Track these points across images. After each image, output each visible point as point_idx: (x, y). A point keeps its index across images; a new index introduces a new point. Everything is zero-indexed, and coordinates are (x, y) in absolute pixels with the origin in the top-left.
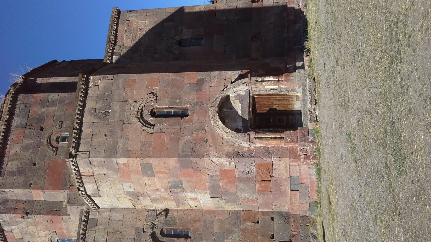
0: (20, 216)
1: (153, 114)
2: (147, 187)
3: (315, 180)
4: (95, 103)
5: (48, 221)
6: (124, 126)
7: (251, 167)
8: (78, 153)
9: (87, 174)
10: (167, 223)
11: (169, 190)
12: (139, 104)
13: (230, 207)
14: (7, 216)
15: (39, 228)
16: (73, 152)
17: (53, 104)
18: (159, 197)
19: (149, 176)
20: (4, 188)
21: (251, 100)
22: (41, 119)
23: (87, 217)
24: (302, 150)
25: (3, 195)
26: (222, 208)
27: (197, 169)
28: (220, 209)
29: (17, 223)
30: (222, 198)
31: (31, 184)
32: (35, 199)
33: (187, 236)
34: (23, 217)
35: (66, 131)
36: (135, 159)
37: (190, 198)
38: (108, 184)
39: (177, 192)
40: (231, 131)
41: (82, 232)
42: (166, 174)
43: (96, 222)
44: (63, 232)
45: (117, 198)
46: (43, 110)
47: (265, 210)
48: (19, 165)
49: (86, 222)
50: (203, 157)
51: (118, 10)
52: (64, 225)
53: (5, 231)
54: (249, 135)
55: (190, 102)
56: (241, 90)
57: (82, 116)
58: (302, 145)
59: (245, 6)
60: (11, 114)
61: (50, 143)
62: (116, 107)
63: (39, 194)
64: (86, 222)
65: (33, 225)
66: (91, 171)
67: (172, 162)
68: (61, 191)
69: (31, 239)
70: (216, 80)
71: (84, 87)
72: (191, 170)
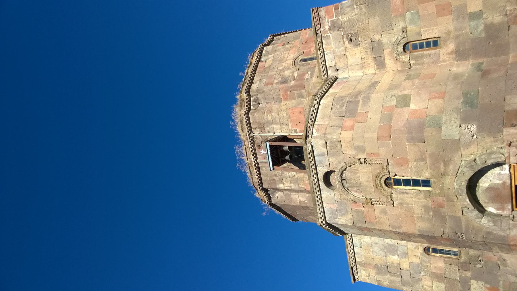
15: (291, 52)
44: (310, 50)
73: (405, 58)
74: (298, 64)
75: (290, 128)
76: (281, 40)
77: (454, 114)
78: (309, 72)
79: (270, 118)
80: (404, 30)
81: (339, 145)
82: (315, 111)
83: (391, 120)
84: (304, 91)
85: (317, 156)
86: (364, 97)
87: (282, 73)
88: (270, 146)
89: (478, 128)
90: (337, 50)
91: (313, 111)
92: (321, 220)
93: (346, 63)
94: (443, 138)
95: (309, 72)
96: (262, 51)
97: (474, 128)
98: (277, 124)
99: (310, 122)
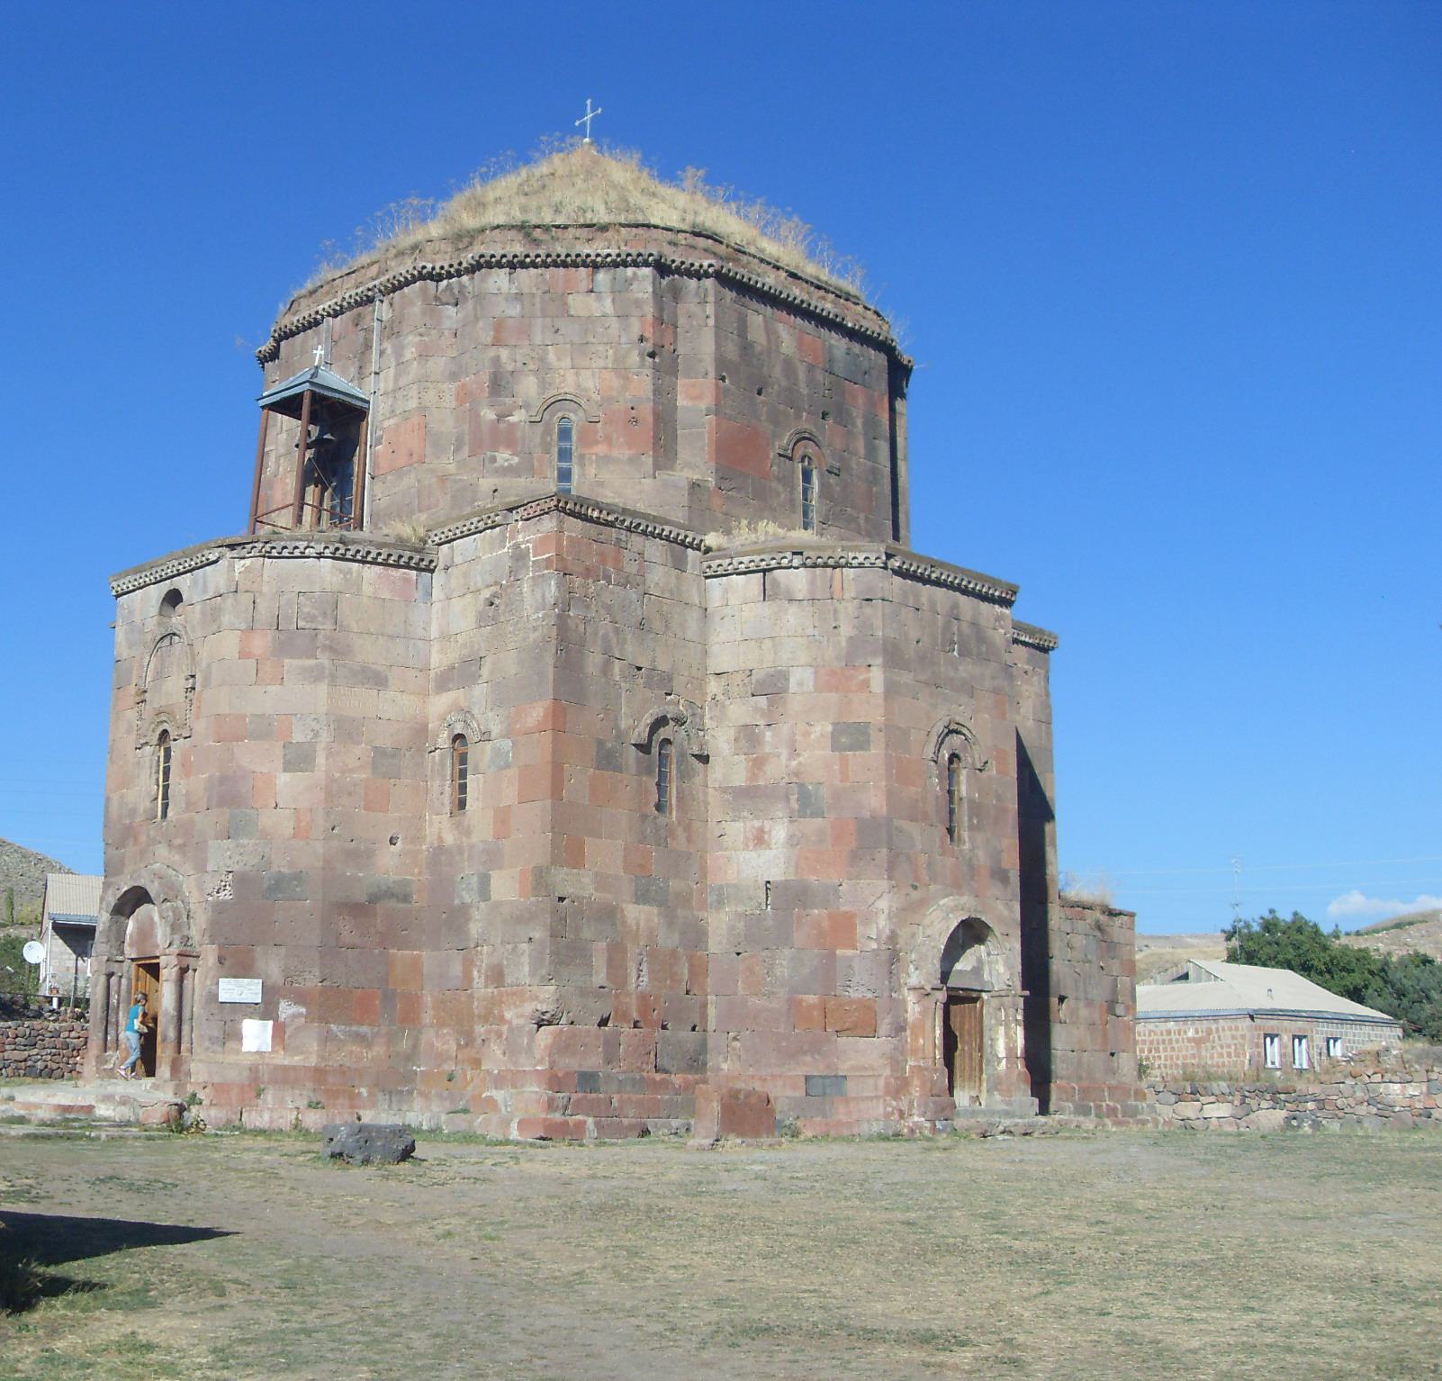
0: (648, 334)
1: (954, 757)
3: (856, 1131)
5: (633, 409)
7: (862, 989)
8: (890, 572)
9: (837, 584)
10: (682, 755)
11: (795, 780)
13: (720, 925)
14: (646, 296)
15: (607, 375)
16: (896, 563)
17: (871, 452)
18: (767, 750)
19: (834, 736)
20: (715, 302)
21: (974, 995)
22: (843, 417)
23: (690, 546)
24: (911, 1103)
25: (693, 292)
26: (715, 904)
28: (712, 898)
29: (623, 316)
30: (767, 905)
31: (723, 379)
32: (681, 382)
33: (659, 807)
34: (641, 339)
35: (822, 485)
36: (881, 711)
37: (766, 830)
38: (810, 631)
39: (789, 799)
40: (943, 947)
42: (841, 781)
43: (679, 565)
44: (596, 442)
45: (760, 641)
46: (859, 422)
47: (712, 1011)
48: (758, 349)
49: (682, 543)
50: (890, 878)
51: (1053, 648)
52: (627, 453)
53: (593, 274)
54: (941, 989)
55: (972, 850)
56: (994, 972)
57: (951, 587)
58: (926, 1104)
59: (1054, 978)
60: (854, 335)
61: (802, 438)
62: (966, 669)
63: (699, 397)
64: (682, 543)
65: (616, 360)
66: (847, 596)
67: (874, 801)
68: (713, 464)
69: (568, 340)
70: (1006, 913)
71: (997, 594)
73: (444, 740)
75: (386, 424)
77: (256, 861)
78: (516, 460)
79: (410, 353)
80: (486, 737)
81: (215, 628)
82: (297, 553)
84: (466, 451)
85: (205, 574)
86: (324, 668)
87: (532, 367)
88: (301, 395)
89: (225, 902)
90: (479, 567)
91: (296, 548)
92: (114, 584)
93: (455, 594)
94: (210, 842)
95: (516, 460)
96: (635, 264)
97: (226, 895)
98: (396, 380)
99: (268, 547)
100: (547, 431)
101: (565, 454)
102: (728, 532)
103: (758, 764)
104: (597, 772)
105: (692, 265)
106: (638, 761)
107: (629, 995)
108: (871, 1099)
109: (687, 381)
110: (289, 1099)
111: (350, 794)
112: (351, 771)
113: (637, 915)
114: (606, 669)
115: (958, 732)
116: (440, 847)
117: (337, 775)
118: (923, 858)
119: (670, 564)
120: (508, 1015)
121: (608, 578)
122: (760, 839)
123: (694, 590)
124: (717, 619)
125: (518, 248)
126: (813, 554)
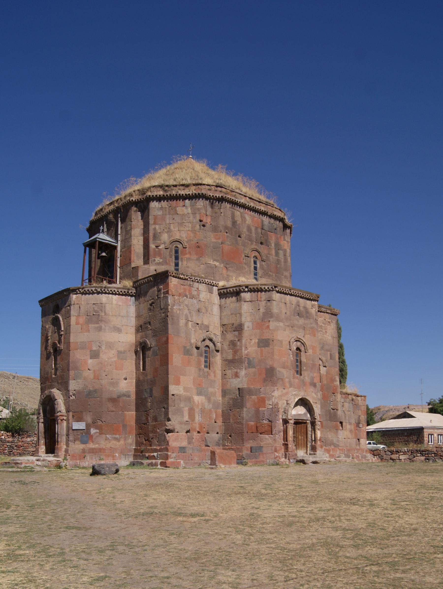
2: (249, 340)
4: (303, 305)
6: (291, 327)
9: (259, 296)
12: (303, 339)
15: (189, 232)
18: (238, 348)
19: (258, 343)
21: (305, 421)
27: (265, 380)
29: (194, 214)
38: (251, 311)
41: (206, 280)
43: (211, 292)
44: (186, 254)
48: (238, 222)
57: (296, 296)
62: (301, 321)
63: (219, 239)
64: (211, 285)
65: (192, 228)
66: (262, 300)
72: (264, 376)
74: (173, 245)
76: (218, 211)
78: (161, 260)
83: (82, 348)
87: (166, 231)
95: (161, 260)
98: (125, 236)
100: (171, 251)
101: (177, 258)
102: (228, 281)
103: (235, 352)
104: (184, 356)
105: (216, 196)
106: (198, 353)
107: (196, 423)
108: (270, 453)
109: (215, 234)
110: (94, 458)
111: (111, 365)
112: (110, 358)
113: (197, 399)
114: (186, 324)
115: (299, 341)
116: (139, 380)
117: (106, 359)
118: (287, 380)
119: (207, 291)
120: (158, 430)
121: (187, 298)
122: (236, 375)
123: (216, 299)
124: (223, 308)
125: (161, 193)
126: (252, 287)
